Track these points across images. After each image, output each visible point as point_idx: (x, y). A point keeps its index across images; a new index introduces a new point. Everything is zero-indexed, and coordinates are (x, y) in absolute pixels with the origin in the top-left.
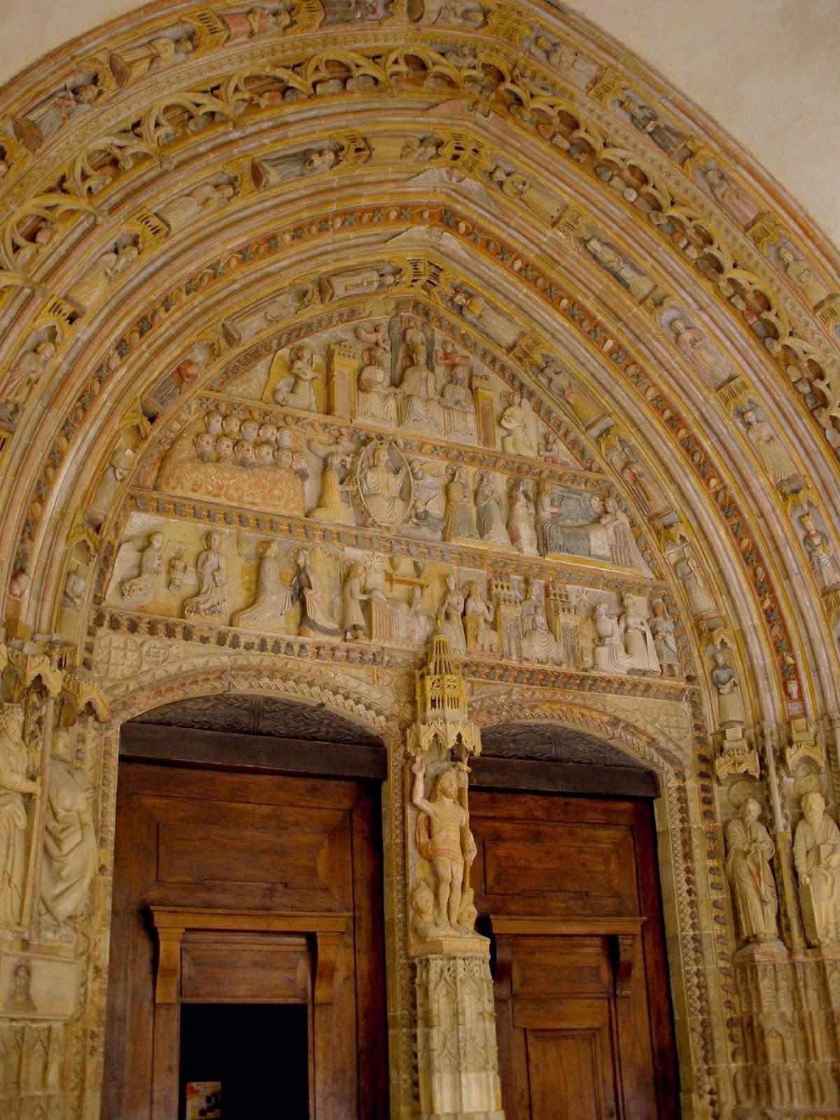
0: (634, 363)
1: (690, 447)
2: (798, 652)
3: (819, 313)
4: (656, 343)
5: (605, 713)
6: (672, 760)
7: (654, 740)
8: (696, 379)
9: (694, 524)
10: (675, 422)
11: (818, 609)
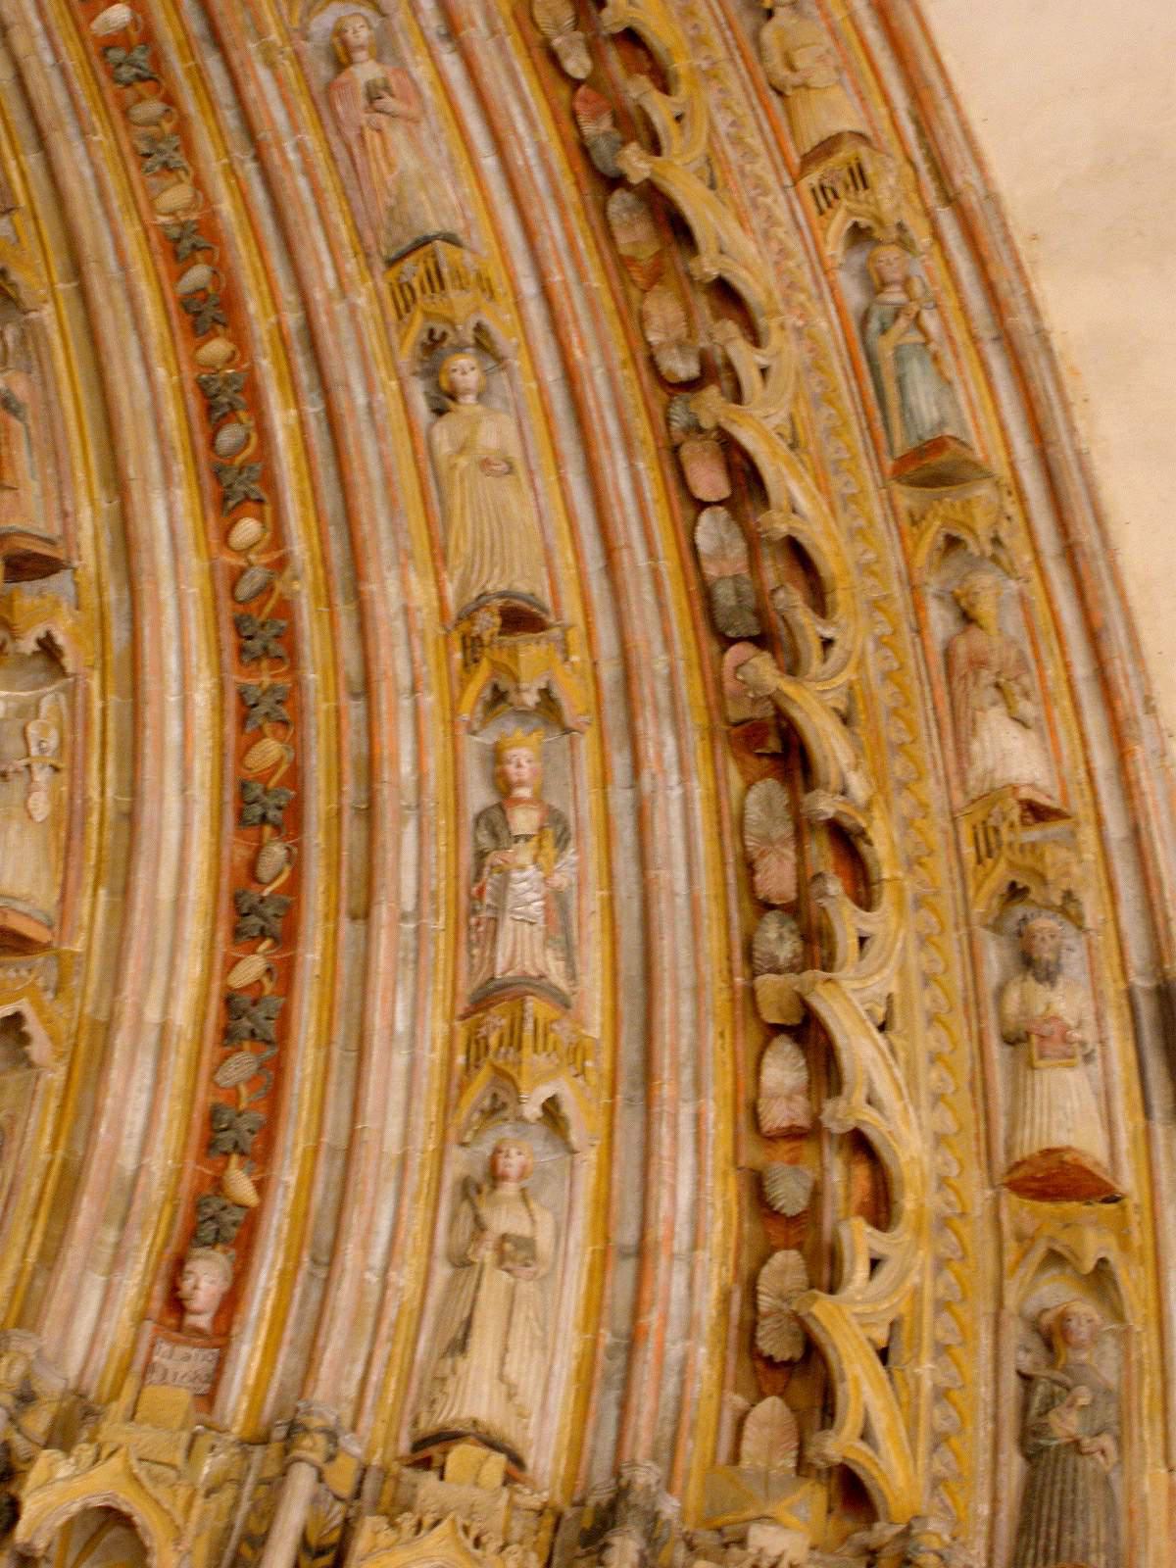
0: (170, 100)
1: (223, 401)
2: (287, 1174)
3: (813, 178)
4: (264, 74)
8: (337, 218)
9: (118, 634)
10: (209, 313)
11: (432, 1057)
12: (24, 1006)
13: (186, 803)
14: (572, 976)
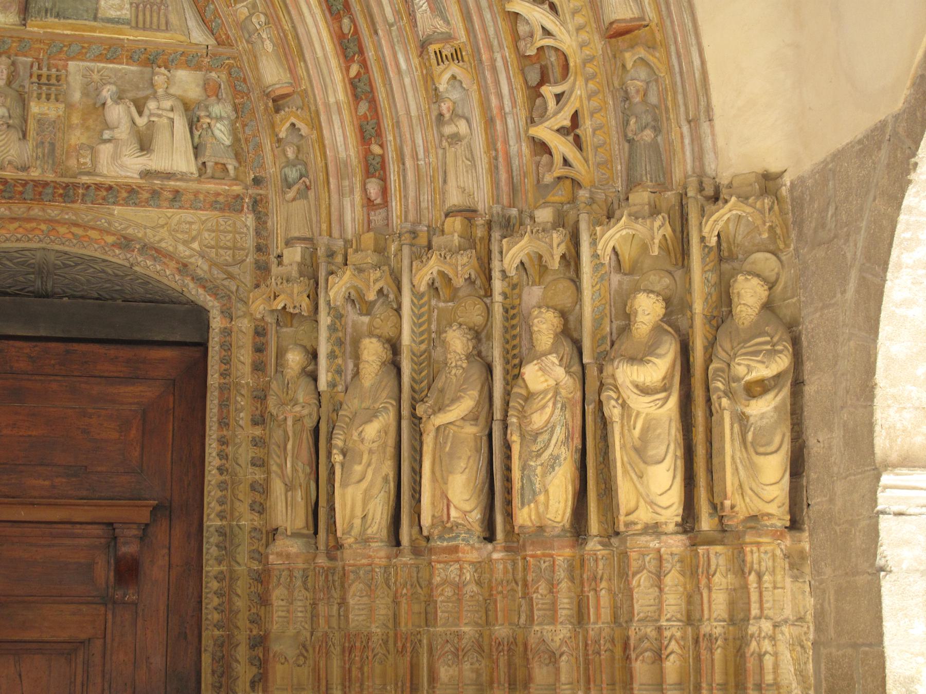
5: (109, 233)
6: (214, 291)
7: (185, 265)
12: (293, 120)
13: (313, 16)
14: (448, 23)
